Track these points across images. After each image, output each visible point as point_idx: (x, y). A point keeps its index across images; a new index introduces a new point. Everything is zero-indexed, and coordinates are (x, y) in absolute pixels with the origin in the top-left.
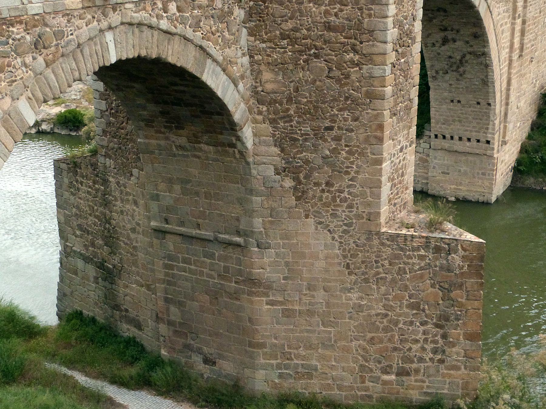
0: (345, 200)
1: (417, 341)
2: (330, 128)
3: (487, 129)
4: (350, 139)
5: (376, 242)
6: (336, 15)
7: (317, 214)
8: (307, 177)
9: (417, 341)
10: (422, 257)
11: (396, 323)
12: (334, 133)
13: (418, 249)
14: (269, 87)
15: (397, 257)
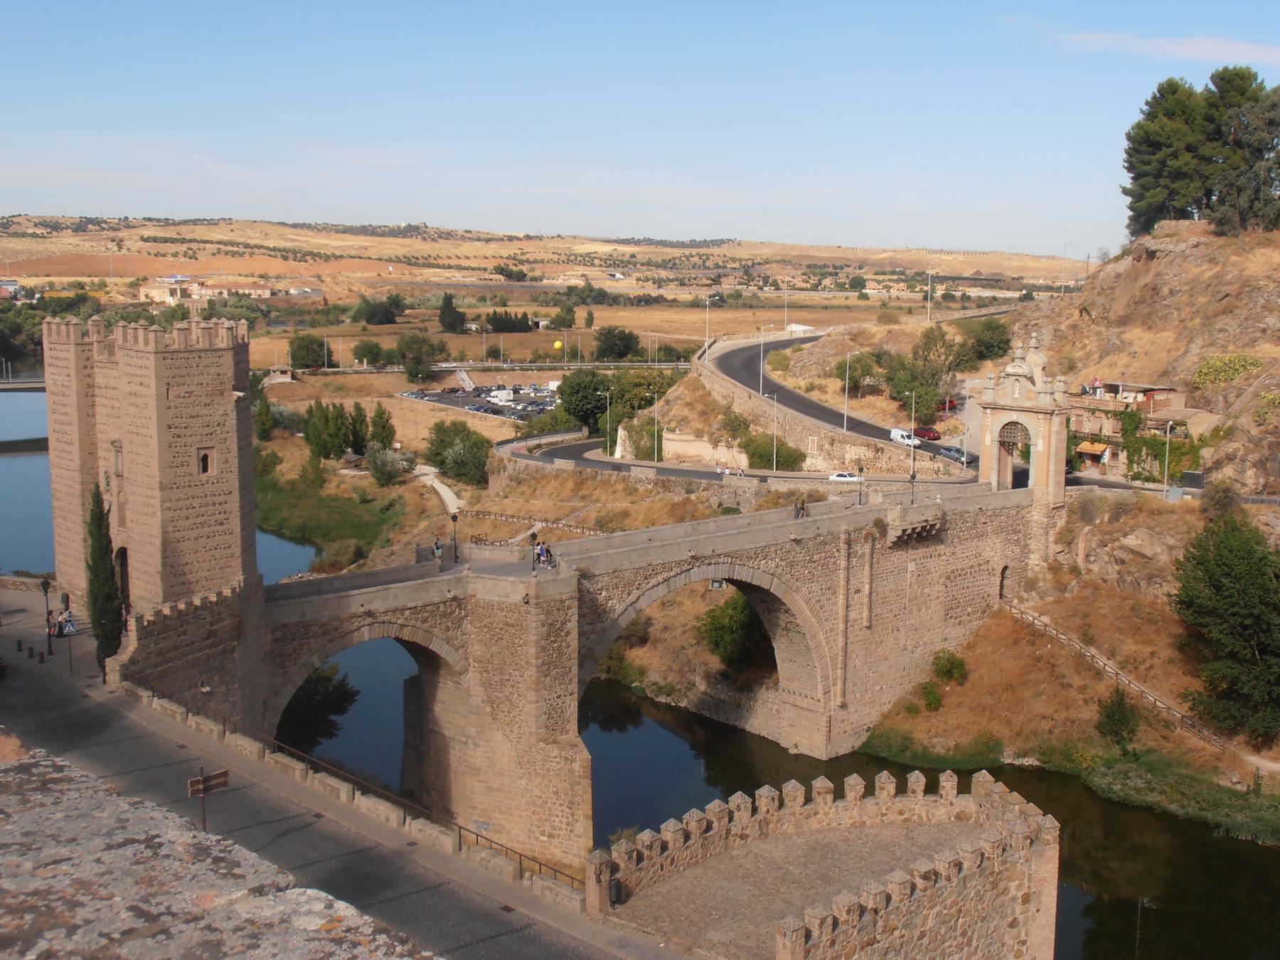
0: (517, 723)
1: (558, 816)
2: (508, 680)
4: (518, 688)
5: (534, 750)
7: (503, 730)
8: (498, 707)
9: (558, 816)
10: (558, 763)
11: (547, 803)
12: (511, 683)
13: (556, 757)
14: (478, 653)
15: (546, 761)
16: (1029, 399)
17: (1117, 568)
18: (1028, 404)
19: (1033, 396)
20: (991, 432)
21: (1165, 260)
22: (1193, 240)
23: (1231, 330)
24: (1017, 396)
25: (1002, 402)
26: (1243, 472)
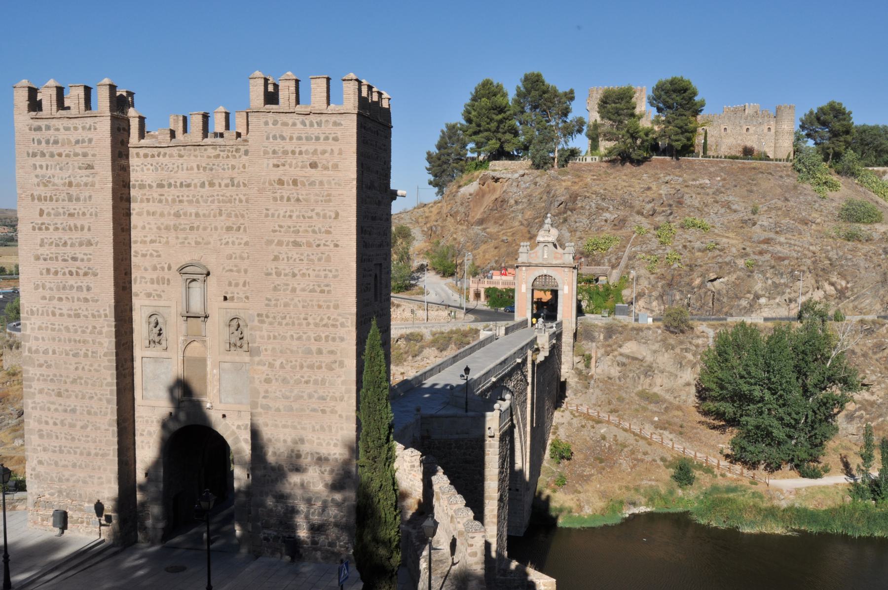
3: (516, 481)
6: (470, 455)
16: (555, 258)
17: (619, 369)
18: (555, 262)
19: (559, 256)
20: (526, 283)
21: (506, 184)
22: (521, 172)
23: (584, 221)
24: (546, 256)
25: (534, 262)
26: (650, 303)
